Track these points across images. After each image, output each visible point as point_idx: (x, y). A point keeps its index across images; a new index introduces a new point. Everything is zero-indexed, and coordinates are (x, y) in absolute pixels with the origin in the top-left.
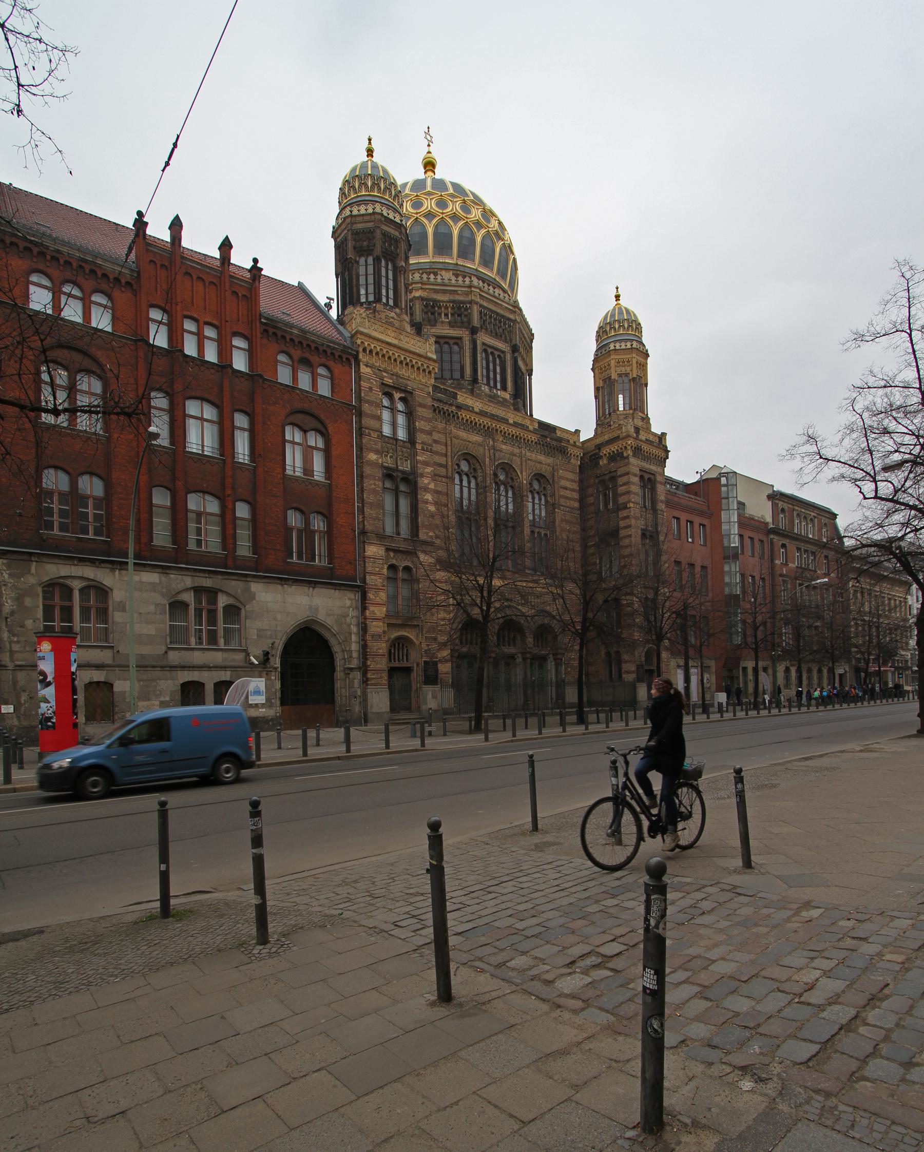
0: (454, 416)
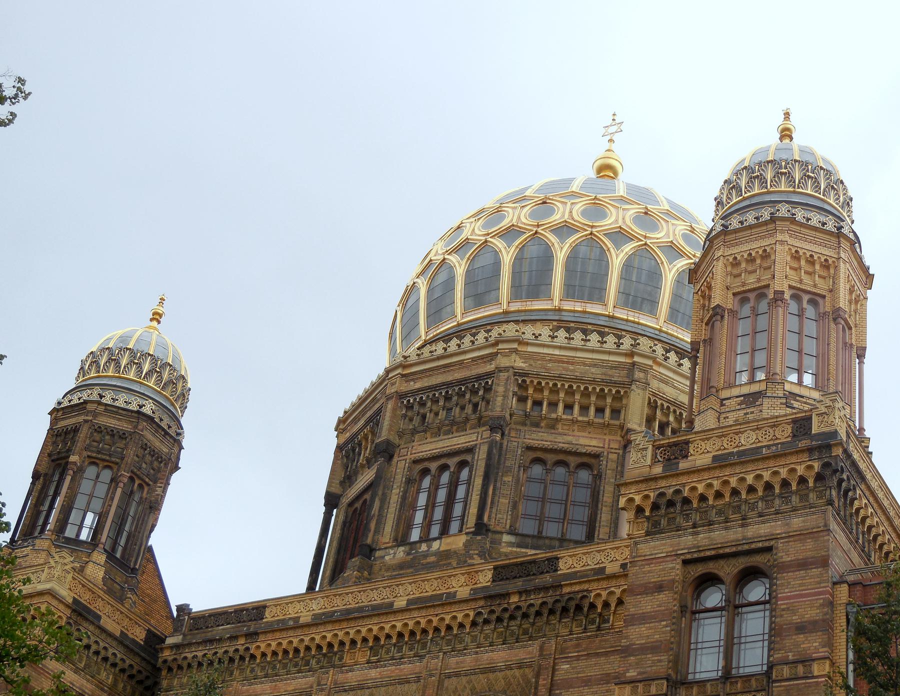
0: (242, 658)
